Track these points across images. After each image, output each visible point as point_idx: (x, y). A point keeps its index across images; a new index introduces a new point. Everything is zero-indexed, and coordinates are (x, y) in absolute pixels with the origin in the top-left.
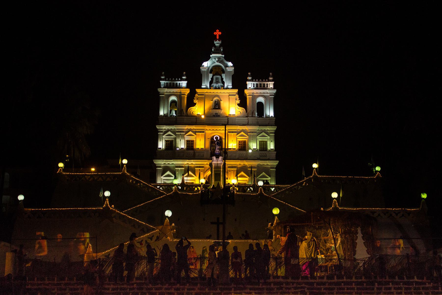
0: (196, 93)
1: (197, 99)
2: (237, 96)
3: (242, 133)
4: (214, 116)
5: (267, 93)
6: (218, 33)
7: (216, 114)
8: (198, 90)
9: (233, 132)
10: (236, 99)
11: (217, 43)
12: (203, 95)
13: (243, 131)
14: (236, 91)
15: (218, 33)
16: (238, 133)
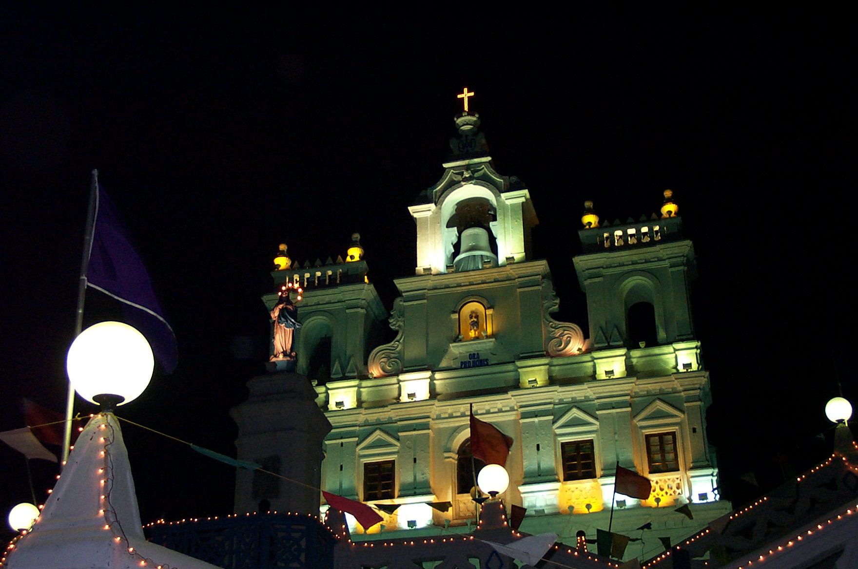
0: (397, 293)
1: (402, 315)
2: (548, 284)
3: (575, 413)
4: (464, 365)
5: (660, 260)
6: (466, 95)
7: (472, 356)
8: (402, 284)
9: (536, 415)
10: (545, 298)
11: (466, 122)
12: (422, 297)
13: (575, 404)
14: (541, 266)
15: (466, 95)
16: (557, 414)
